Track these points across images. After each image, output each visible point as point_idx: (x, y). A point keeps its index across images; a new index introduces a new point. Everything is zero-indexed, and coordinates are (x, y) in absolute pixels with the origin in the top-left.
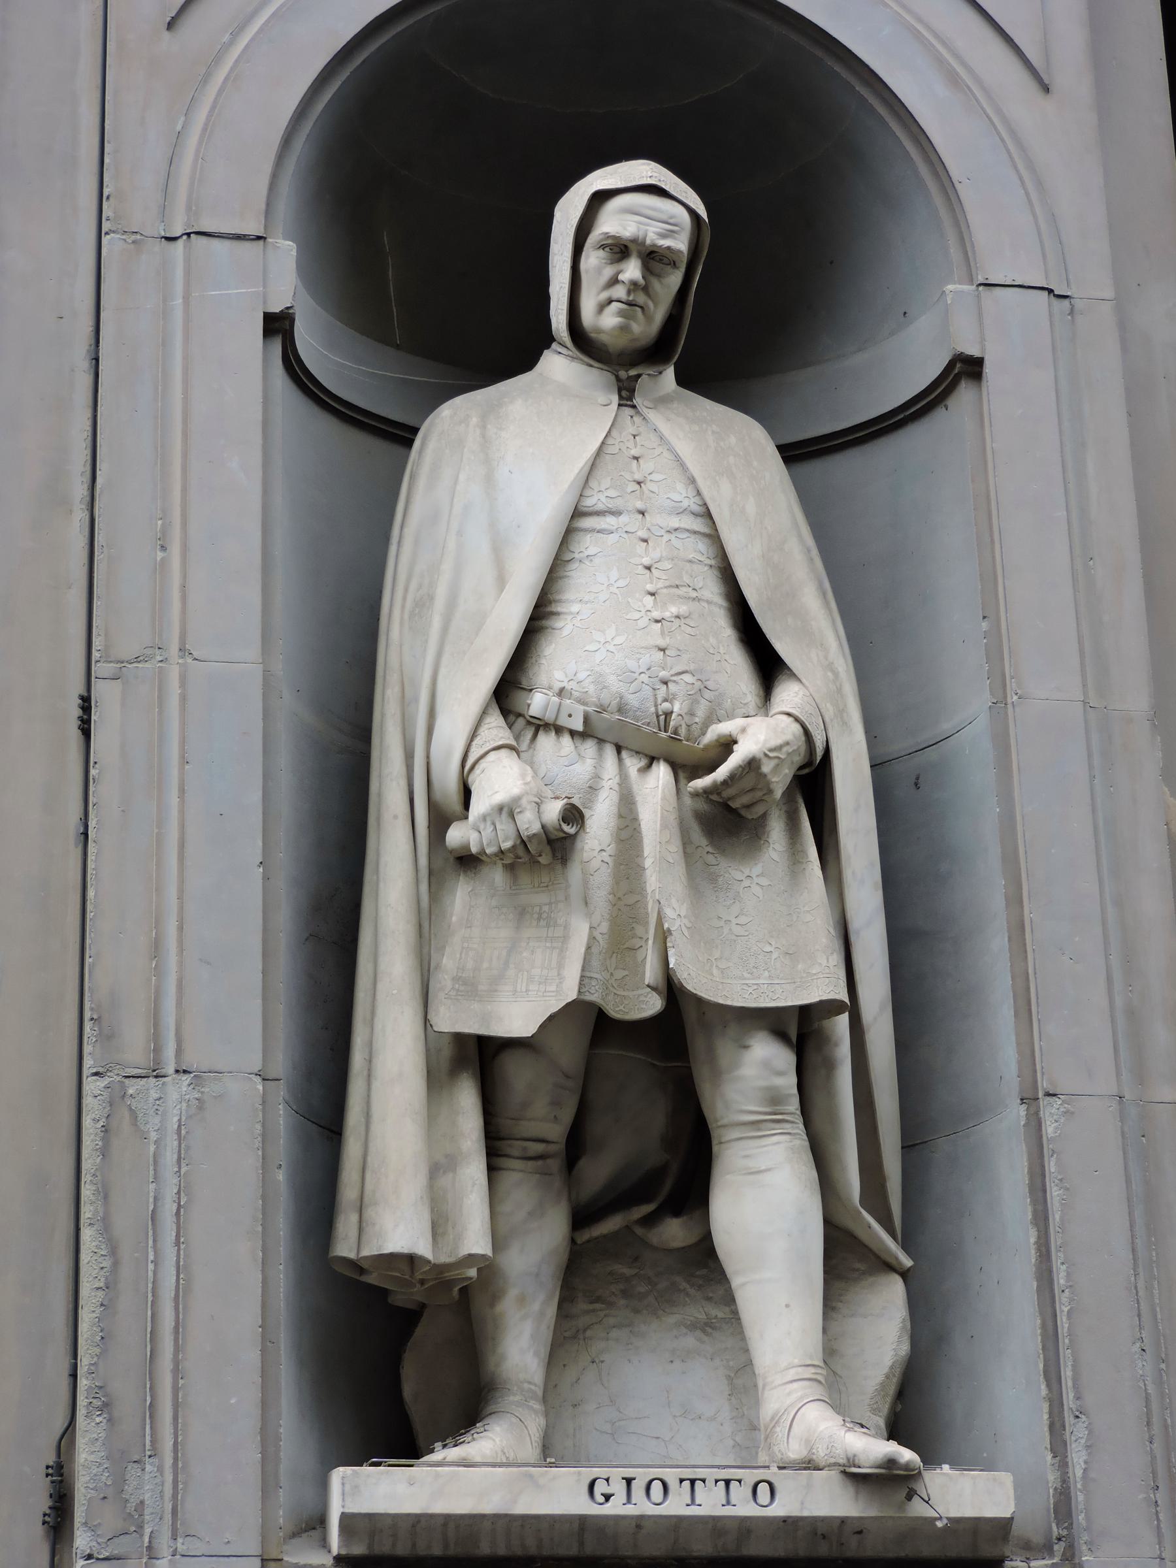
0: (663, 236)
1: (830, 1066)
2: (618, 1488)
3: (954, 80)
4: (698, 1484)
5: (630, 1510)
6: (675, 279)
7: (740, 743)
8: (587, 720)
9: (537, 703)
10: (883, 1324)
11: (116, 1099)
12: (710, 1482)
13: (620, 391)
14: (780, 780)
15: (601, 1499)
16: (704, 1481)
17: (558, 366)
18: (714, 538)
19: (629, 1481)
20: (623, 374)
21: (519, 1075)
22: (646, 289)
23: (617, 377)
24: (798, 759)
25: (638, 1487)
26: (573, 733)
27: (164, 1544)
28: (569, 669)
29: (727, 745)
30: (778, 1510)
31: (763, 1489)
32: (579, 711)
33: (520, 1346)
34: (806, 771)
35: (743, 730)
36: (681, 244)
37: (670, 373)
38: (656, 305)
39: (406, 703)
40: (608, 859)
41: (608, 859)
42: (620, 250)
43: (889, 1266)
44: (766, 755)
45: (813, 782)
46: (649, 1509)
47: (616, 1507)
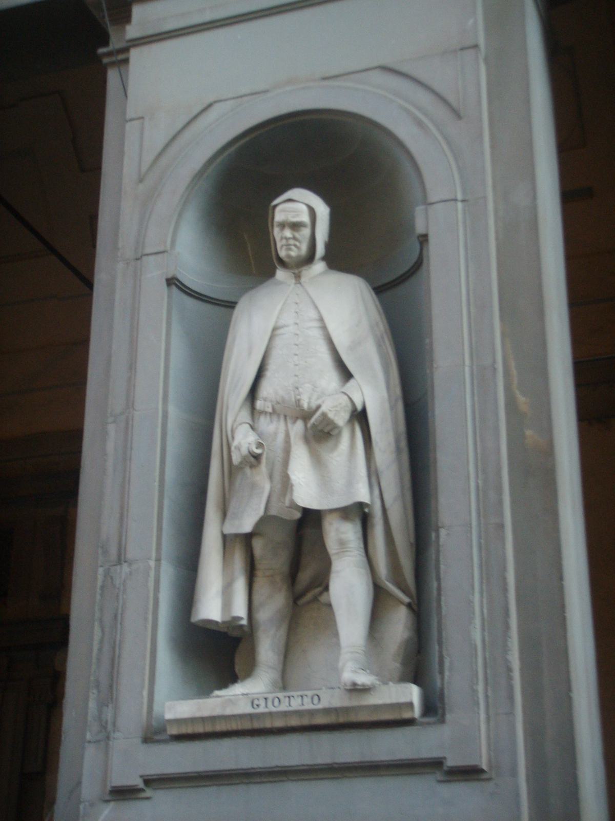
0: (293, 217)
1: (373, 526)
2: (262, 703)
3: (420, 124)
4: (292, 698)
5: (266, 710)
6: (306, 232)
7: (323, 406)
8: (274, 409)
9: (259, 404)
10: (399, 625)
11: (107, 574)
12: (296, 697)
13: (295, 277)
14: (341, 418)
15: (255, 706)
16: (293, 697)
17: (280, 274)
18: (324, 328)
19: (266, 699)
20: (296, 271)
21: (258, 545)
22: (294, 238)
23: (294, 273)
24: (350, 408)
25: (270, 703)
26: (270, 413)
27: (112, 735)
28: (267, 390)
29: (318, 407)
30: (320, 706)
31: (316, 698)
32: (269, 405)
33: (267, 650)
34: (355, 413)
35: (323, 402)
36: (305, 218)
37: (319, 267)
38: (300, 242)
39: (221, 414)
40: (280, 460)
41: (280, 460)
42: (283, 225)
43: (402, 603)
44: (330, 410)
45: (360, 417)
46: (273, 709)
47: (262, 709)
